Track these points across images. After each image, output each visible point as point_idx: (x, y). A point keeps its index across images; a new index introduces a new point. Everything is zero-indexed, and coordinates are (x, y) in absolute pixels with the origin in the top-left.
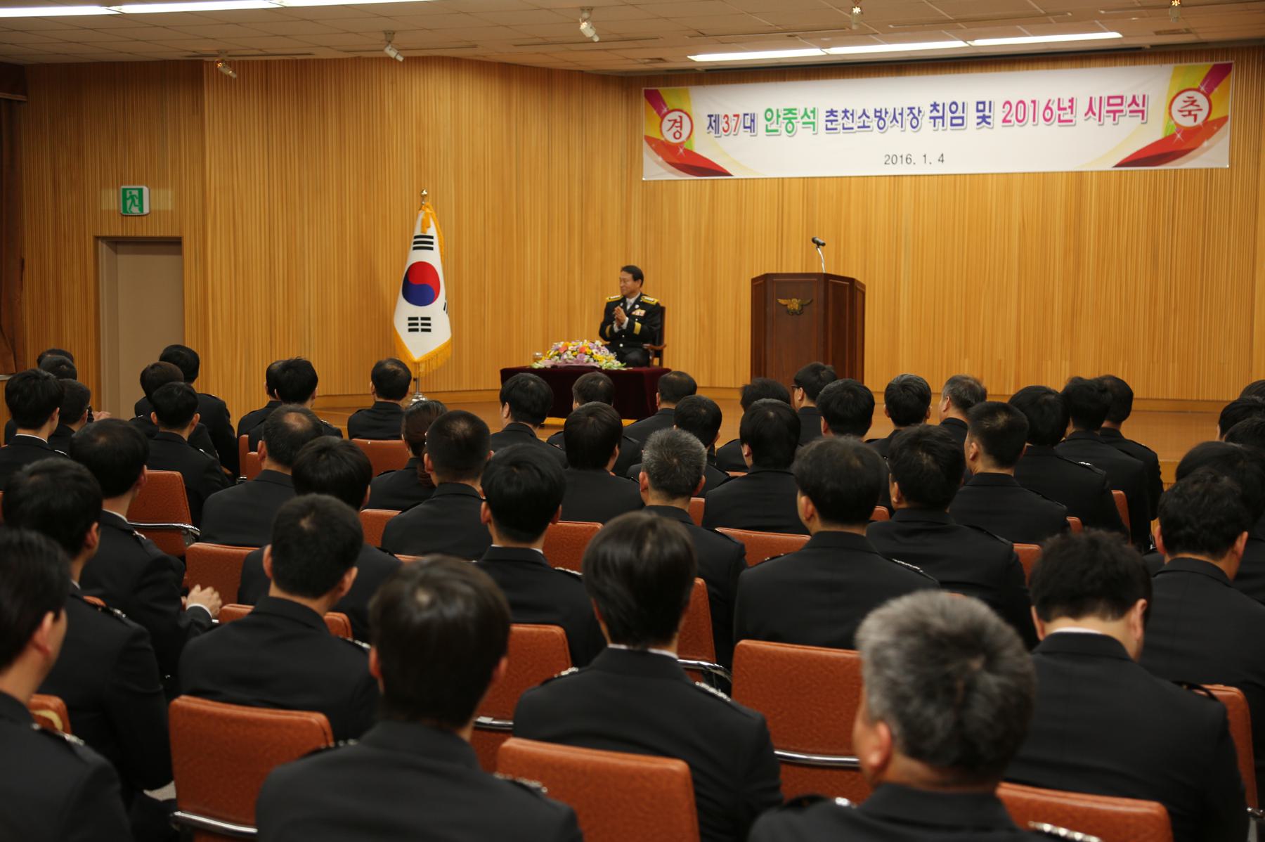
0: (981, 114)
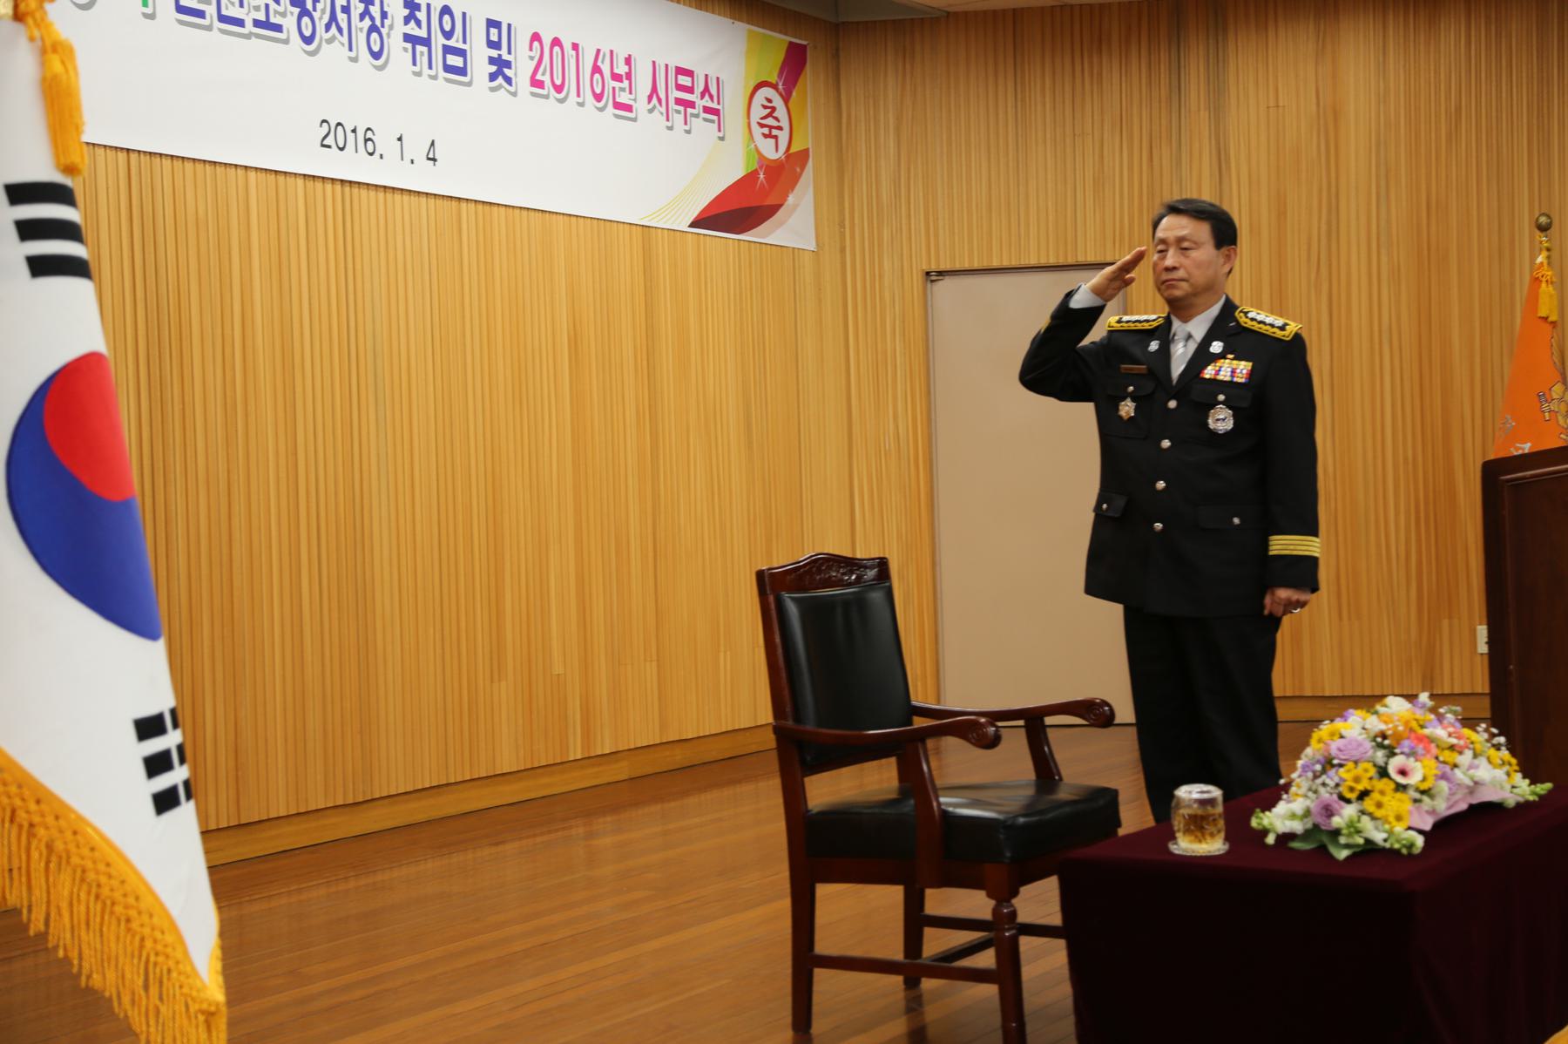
0: (494, 53)
